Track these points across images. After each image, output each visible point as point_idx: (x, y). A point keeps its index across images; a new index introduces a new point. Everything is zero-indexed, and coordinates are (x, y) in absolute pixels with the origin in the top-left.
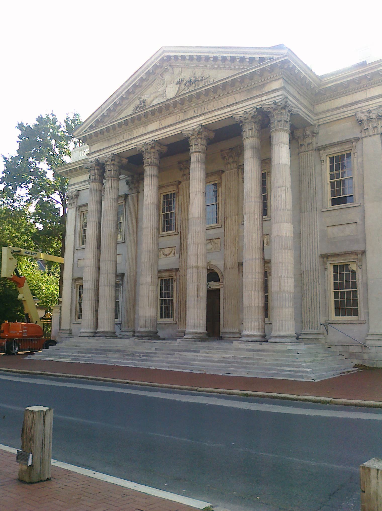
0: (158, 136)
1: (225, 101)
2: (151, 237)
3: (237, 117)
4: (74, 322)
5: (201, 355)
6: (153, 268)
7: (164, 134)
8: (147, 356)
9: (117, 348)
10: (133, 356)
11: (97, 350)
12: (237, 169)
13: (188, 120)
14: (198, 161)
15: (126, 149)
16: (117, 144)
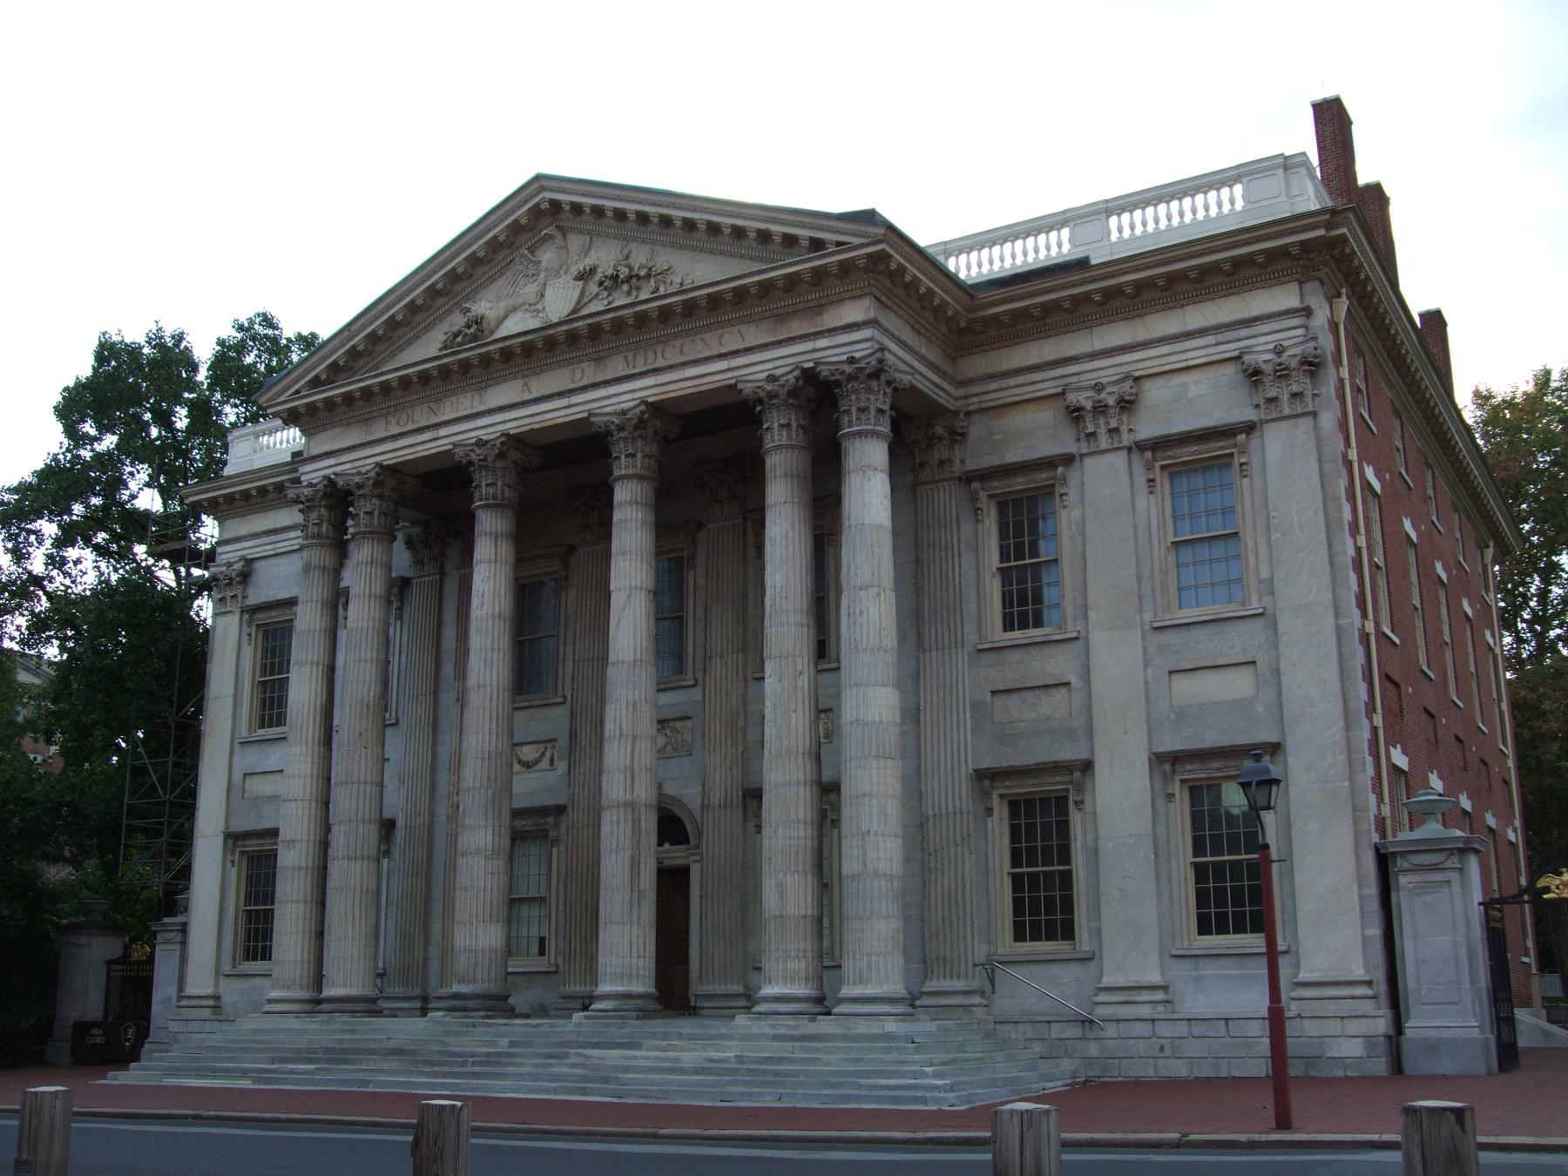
0: (516, 422)
1: (712, 343)
2: (494, 713)
3: (747, 388)
4: (227, 968)
5: (645, 1055)
6: (497, 806)
7: (537, 419)
8: (487, 1064)
9: (391, 1044)
10: (445, 1064)
11: (327, 1050)
12: (741, 520)
13: (607, 383)
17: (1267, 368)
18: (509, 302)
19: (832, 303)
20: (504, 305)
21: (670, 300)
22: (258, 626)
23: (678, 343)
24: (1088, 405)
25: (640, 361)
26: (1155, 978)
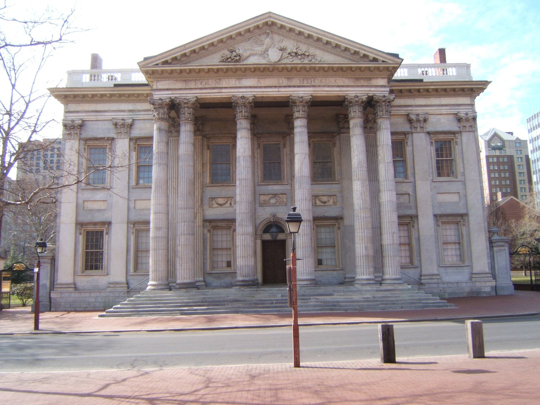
1: (332, 81)
7: (264, 93)
14: (246, 118)
16: (201, 89)
17: (464, 118)
18: (251, 52)
19: (374, 78)
20: (248, 53)
21: (324, 65)
22: (88, 146)
24: (415, 119)
26: (436, 272)
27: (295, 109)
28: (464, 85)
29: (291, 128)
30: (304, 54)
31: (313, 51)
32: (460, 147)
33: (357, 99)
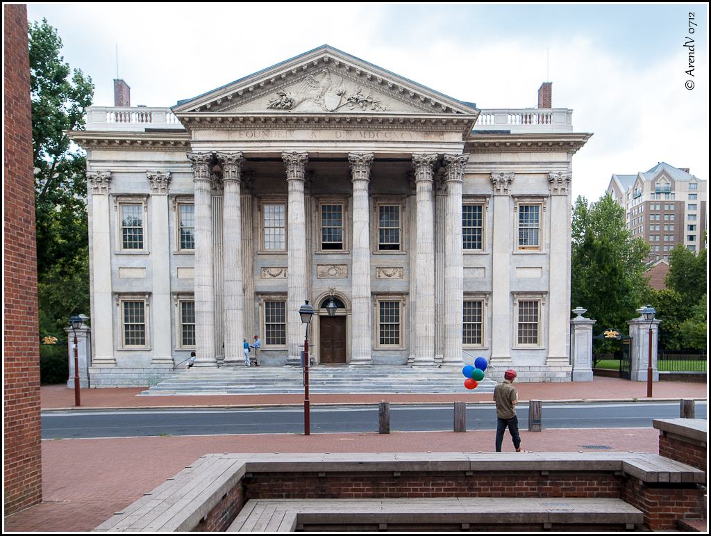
15: (260, 150)
17: (556, 179)
20: (301, 97)
23: (384, 132)
25: (367, 135)
27: (354, 169)
28: (559, 138)
29: (348, 196)
30: (366, 101)
31: (376, 97)
32: (548, 214)
33: (425, 158)
